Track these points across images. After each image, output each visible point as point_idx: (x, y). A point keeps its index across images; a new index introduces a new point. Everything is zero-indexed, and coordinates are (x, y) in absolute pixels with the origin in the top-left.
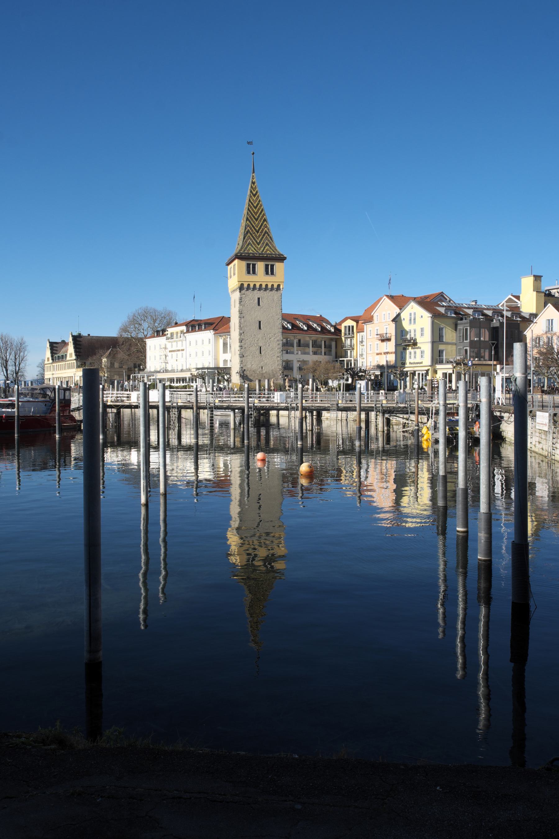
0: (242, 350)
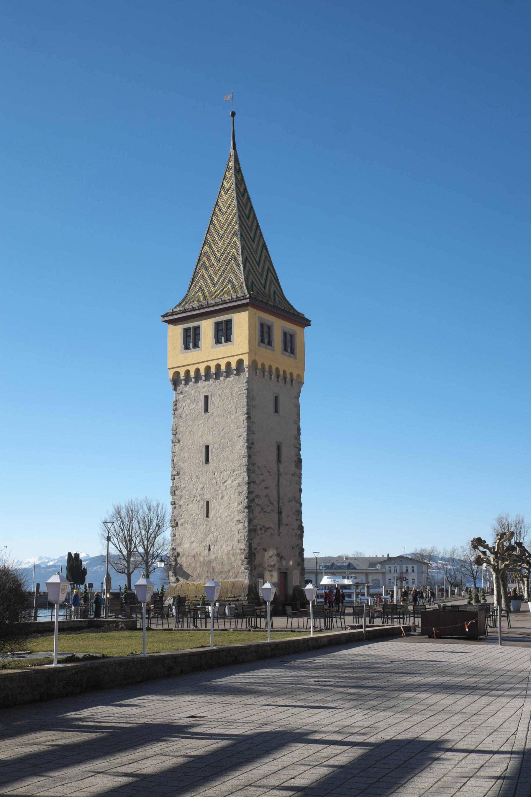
0: (176, 512)
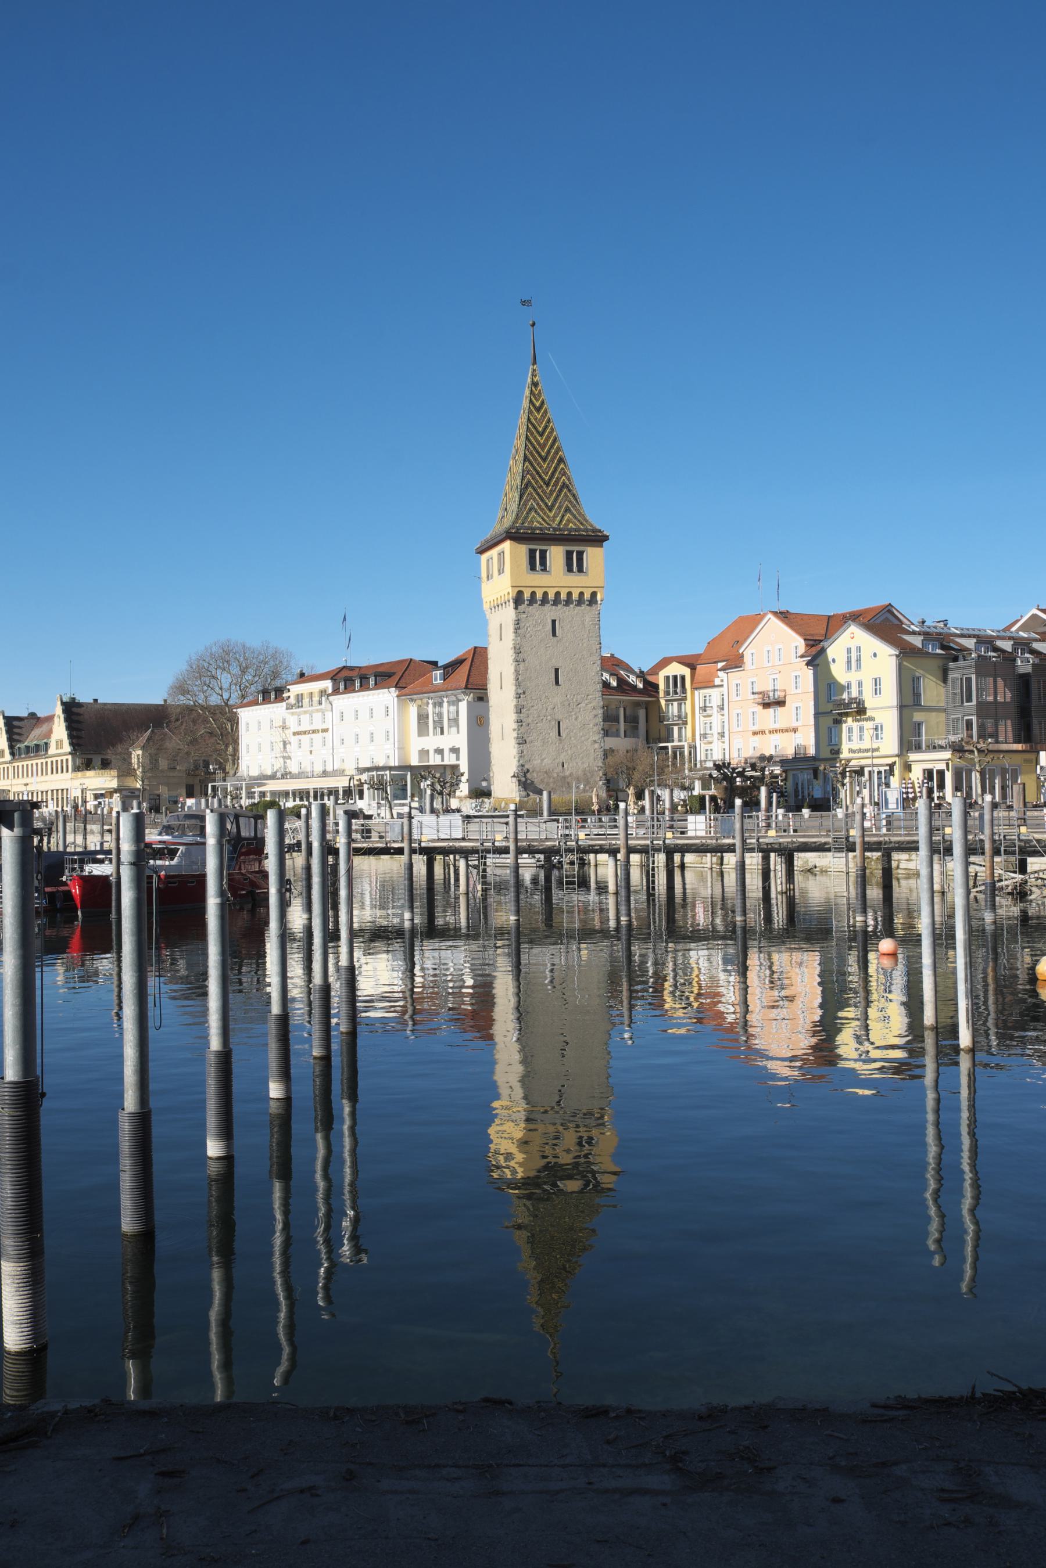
0: (522, 730)
